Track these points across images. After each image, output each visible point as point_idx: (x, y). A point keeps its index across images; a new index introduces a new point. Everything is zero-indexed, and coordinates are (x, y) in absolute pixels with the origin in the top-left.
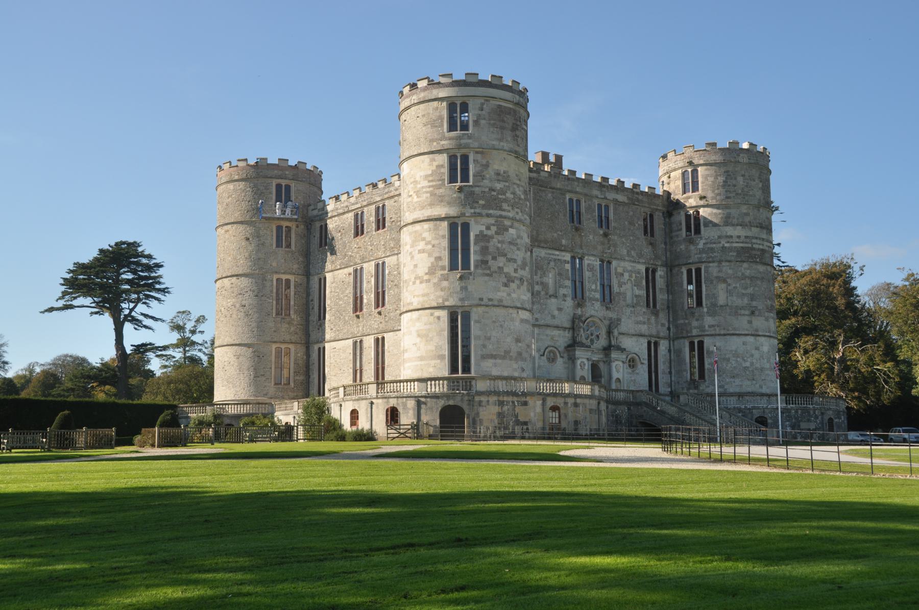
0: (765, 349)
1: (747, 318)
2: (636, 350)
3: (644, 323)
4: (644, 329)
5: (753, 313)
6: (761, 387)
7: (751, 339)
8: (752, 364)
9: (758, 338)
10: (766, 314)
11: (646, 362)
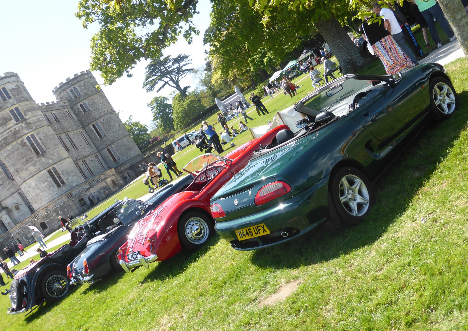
0: (33, 185)
1: (18, 176)
2: (15, 201)
3: (11, 187)
4: (13, 190)
5: (17, 171)
6: (41, 203)
7: (24, 184)
8: (32, 195)
9: (27, 182)
10: (24, 168)
11: (23, 203)
